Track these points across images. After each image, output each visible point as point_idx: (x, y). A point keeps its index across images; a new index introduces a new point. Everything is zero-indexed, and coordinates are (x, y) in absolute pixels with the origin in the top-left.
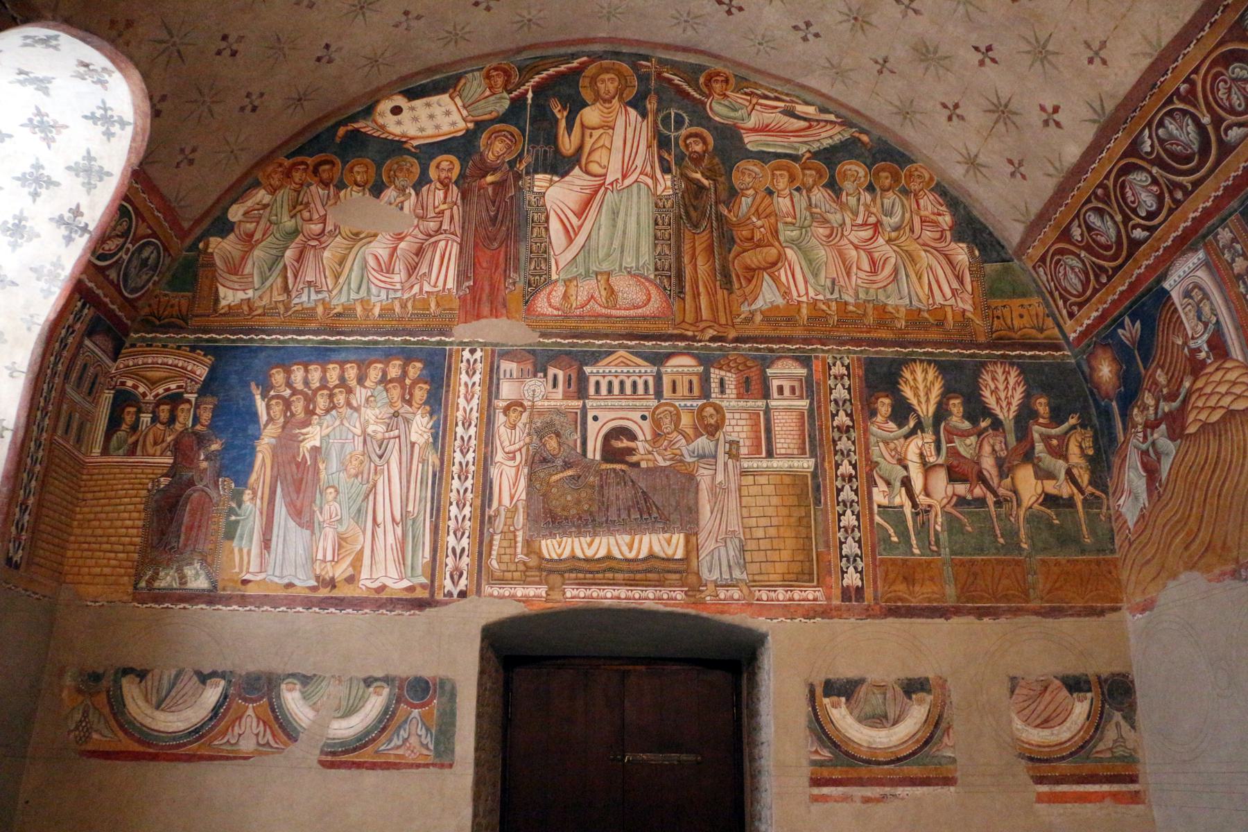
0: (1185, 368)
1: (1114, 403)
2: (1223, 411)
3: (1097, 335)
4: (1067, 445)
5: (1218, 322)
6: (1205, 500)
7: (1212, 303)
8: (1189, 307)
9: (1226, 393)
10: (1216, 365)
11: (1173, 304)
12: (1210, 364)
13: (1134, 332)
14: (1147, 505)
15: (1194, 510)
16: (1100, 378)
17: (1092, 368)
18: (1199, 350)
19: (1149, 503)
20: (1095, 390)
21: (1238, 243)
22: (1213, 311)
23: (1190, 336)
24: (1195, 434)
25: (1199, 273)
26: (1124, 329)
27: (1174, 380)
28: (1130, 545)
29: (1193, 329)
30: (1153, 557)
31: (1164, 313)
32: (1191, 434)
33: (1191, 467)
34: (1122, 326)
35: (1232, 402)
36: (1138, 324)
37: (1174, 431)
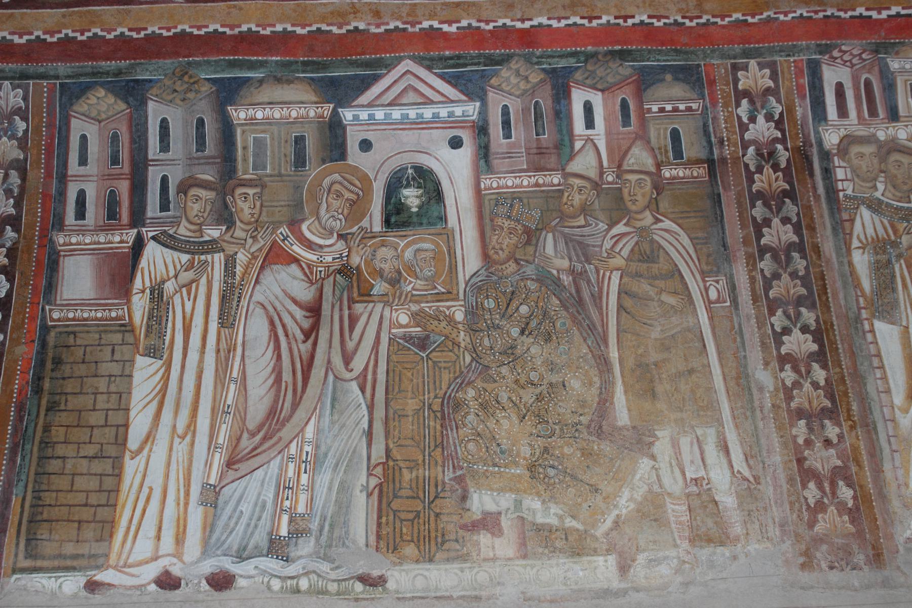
21: (25, 119)
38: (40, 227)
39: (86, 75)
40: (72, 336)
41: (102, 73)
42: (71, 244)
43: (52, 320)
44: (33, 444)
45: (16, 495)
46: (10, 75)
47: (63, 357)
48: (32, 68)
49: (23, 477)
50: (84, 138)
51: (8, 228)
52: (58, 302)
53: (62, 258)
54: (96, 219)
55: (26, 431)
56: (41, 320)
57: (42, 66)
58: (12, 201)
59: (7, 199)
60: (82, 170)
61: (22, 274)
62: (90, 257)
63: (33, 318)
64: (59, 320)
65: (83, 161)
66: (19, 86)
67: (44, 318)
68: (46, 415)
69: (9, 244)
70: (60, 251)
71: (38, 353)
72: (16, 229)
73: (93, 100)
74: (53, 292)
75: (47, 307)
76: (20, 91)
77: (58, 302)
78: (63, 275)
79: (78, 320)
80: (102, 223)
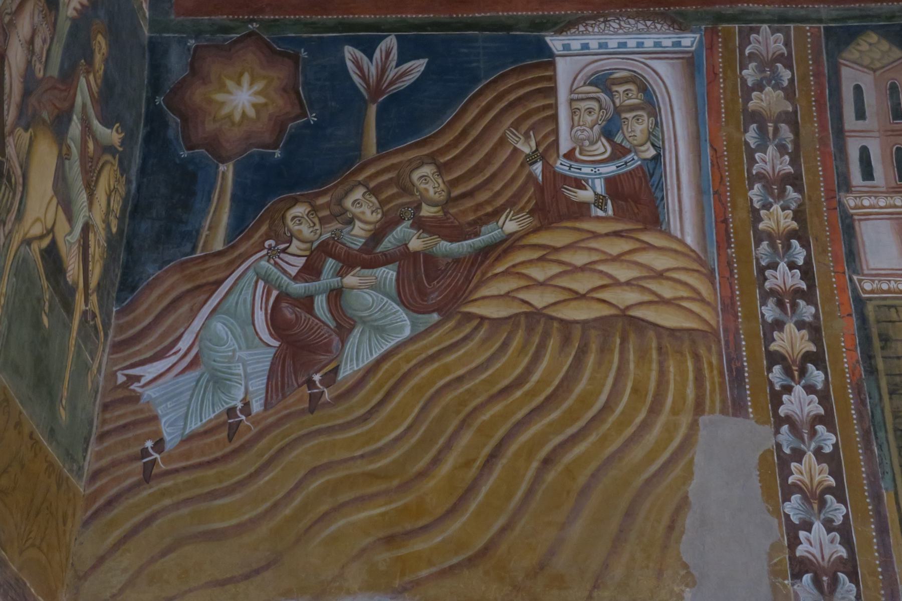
0: (517, 196)
1: (227, 170)
2: (606, 311)
3: (269, 25)
4: (100, 172)
5: (657, 159)
6: (493, 456)
7: (658, 124)
8: (594, 105)
9: (628, 283)
10: (619, 226)
11: (553, 78)
12: (598, 218)
13: (391, 74)
14: (257, 407)
15: (445, 468)
16: (210, 101)
17: (195, 70)
18: (579, 184)
19: (267, 405)
20: (173, 119)
21: (789, 66)
22: (654, 137)
23: (564, 148)
24: (497, 323)
25: (661, 67)
26: (371, 57)
27: (469, 203)
28: (148, 475)
29: (575, 139)
30: (241, 529)
31: (511, 82)
32: (483, 318)
33: (460, 379)
34: (368, 49)
35: (641, 304)
36: (419, 66)
37: (423, 293)
38: (824, 187)
39: (854, 18)
40: (893, 310)
41: (872, 16)
42: (865, 207)
43: (866, 292)
44: (886, 431)
45: (887, 490)
46: (767, 17)
47: (891, 333)
48: (791, 10)
49: (888, 469)
50: (858, 89)
51: (789, 187)
52: (866, 272)
53: (857, 223)
54: (886, 179)
55: (873, 416)
56: (852, 291)
57: (802, 8)
58: (787, 158)
59: (782, 155)
60: (860, 125)
61: (816, 239)
62: (888, 221)
63: (842, 290)
64: (872, 292)
65: (860, 114)
66: (778, 30)
67: (854, 289)
68: (891, 399)
69: (794, 206)
70: (852, 215)
71: (859, 329)
72: (799, 189)
73: (864, 47)
74: (857, 260)
75: (855, 278)
76: (780, 35)
77: (866, 272)
78: (863, 242)
79: (895, 293)
80: (894, 184)
